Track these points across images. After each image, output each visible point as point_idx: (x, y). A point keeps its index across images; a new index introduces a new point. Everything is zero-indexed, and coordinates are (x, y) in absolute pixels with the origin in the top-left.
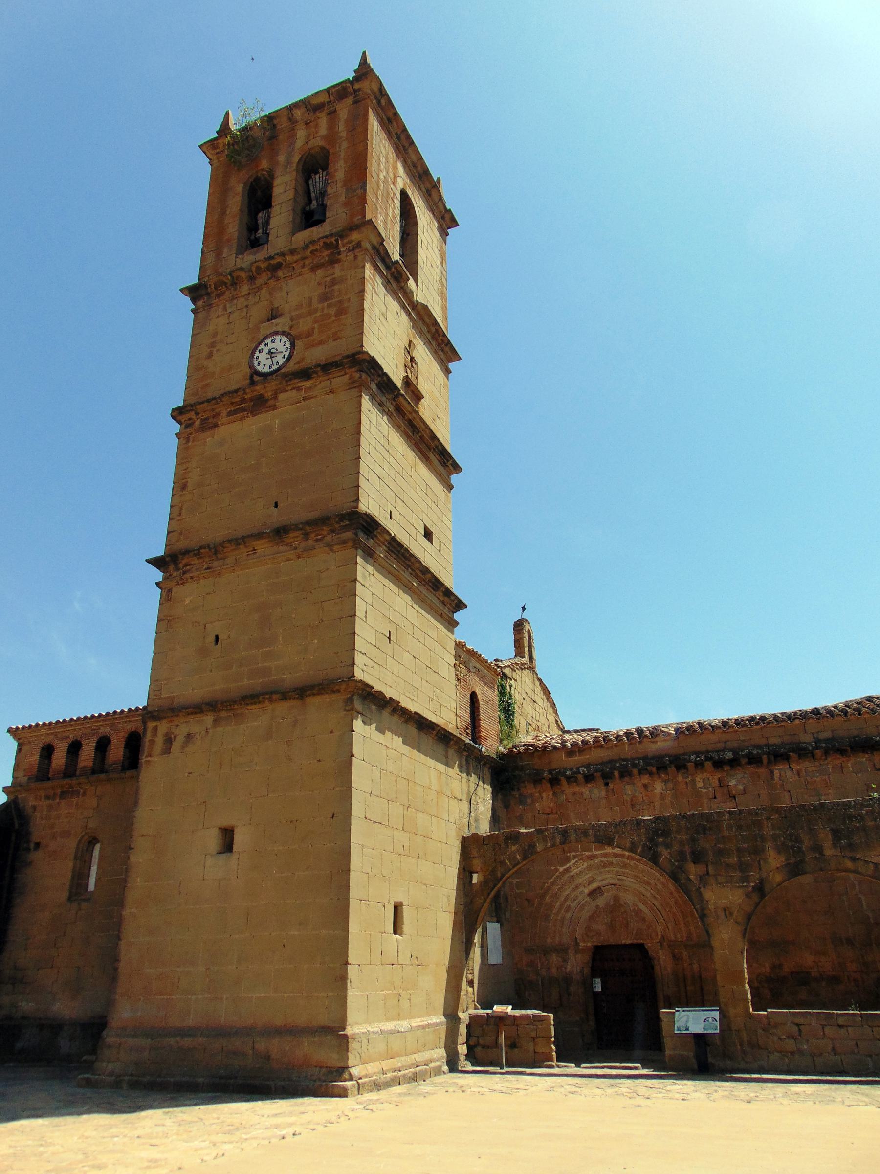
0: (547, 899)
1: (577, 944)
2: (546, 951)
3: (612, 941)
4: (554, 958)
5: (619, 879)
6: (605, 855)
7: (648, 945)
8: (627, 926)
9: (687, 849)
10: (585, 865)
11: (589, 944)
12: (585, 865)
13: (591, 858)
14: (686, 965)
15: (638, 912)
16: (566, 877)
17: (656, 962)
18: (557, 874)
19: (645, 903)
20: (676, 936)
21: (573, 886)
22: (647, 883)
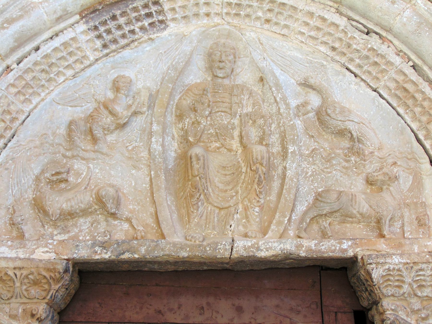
11: (43, 254)
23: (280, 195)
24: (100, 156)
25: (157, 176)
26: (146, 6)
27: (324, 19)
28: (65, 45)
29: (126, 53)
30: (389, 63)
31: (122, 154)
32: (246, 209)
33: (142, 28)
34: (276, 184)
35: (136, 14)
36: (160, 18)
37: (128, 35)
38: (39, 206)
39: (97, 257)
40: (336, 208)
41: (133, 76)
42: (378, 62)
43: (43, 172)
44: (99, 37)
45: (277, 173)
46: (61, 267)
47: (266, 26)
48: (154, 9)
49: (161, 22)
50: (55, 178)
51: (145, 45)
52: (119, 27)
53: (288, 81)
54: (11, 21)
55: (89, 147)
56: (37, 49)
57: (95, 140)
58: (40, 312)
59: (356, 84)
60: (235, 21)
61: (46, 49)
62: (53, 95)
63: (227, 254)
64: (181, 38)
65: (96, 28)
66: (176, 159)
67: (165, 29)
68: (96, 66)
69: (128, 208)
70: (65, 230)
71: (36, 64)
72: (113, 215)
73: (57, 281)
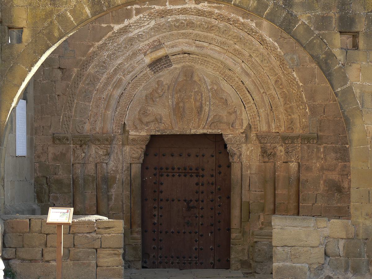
0: (91, 69)
2: (84, 141)
3: (177, 130)
4: (94, 151)
5: (197, 46)
6: (184, 11)
7: (228, 136)
8: (200, 109)
9: (334, 14)
10: (153, 23)
11: (143, 133)
13: (163, 14)
14: (279, 163)
15: (217, 93)
16: (122, 39)
17: (236, 159)
18: (110, 34)
19: (228, 79)
20: (269, 126)
21: (130, 53)
22: (237, 53)
24: (155, 106)
29: (161, 73)
31: (161, 105)
32: (195, 119)
34: (203, 112)
35: (163, 63)
38: (140, 120)
39: (157, 134)
41: (163, 80)
43: (140, 110)
46: (149, 137)
50: (144, 112)
51: (166, 71)
52: (158, 67)
53: (208, 80)
54: (130, 72)
56: (136, 76)
57: (153, 101)
58: (144, 147)
59: (227, 84)
63: (189, 134)
64: (176, 68)
66: (176, 104)
67: (171, 66)
70: (147, 126)
72: (160, 123)
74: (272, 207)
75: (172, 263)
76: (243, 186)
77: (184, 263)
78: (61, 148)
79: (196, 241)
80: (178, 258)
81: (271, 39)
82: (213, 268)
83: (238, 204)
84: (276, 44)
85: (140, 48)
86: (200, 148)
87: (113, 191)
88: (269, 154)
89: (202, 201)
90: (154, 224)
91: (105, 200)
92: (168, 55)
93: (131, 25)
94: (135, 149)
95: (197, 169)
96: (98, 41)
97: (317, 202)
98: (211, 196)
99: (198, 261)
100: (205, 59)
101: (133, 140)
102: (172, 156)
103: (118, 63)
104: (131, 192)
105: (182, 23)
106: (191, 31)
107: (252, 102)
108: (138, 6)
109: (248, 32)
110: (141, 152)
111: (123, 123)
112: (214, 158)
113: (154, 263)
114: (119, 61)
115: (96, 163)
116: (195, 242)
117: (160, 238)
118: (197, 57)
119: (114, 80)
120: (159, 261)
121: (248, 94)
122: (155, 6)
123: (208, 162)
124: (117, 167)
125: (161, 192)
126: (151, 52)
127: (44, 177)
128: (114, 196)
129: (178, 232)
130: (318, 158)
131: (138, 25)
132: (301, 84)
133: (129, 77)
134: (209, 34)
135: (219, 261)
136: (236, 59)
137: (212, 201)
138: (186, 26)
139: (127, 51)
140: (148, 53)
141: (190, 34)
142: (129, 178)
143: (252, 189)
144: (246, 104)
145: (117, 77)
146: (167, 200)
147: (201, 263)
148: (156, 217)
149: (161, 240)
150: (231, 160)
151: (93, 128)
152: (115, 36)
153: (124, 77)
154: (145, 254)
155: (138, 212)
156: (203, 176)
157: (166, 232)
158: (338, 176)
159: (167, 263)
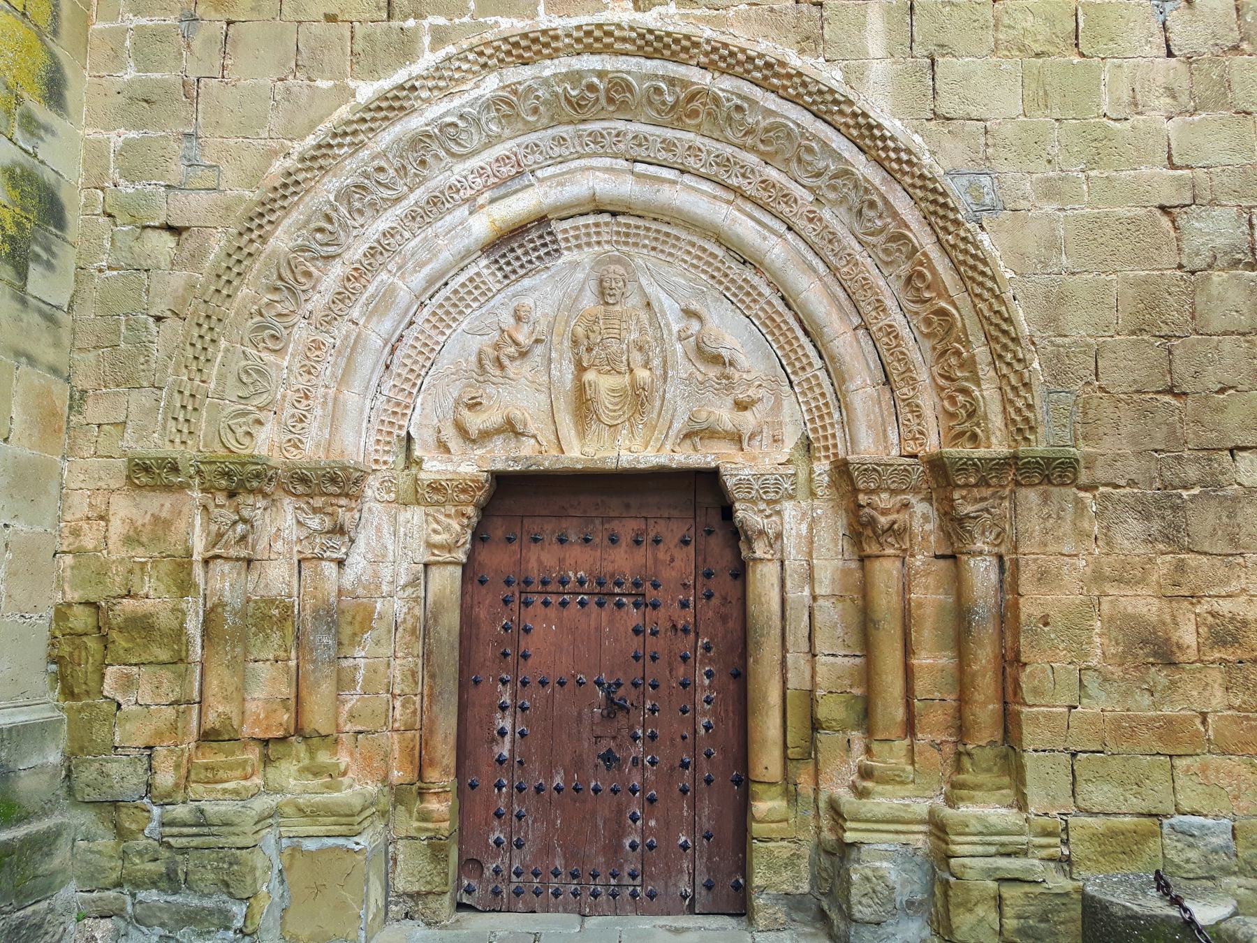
0: (281, 240)
1: (411, 461)
10: (491, 84)
12: (491, 84)
16: (387, 137)
21: (420, 195)
23: (660, 414)
25: (557, 399)
26: (541, 237)
27: (705, 250)
28: (471, 280)
29: (526, 282)
30: (760, 294)
33: (539, 258)
36: (555, 247)
37: (527, 265)
40: (704, 426)
41: (532, 305)
42: (752, 293)
44: (500, 269)
45: (657, 396)
47: (653, 253)
48: (548, 239)
49: (556, 251)
52: (518, 258)
54: (422, 265)
55: (498, 373)
56: (446, 284)
57: (502, 367)
60: (624, 248)
61: (454, 285)
62: (463, 326)
63: (613, 466)
64: (575, 265)
65: (496, 262)
68: (499, 296)
69: (532, 428)
71: (448, 299)
72: (522, 434)
73: (480, 489)
74: (900, 714)
75: (556, 894)
76: (790, 639)
77: (595, 895)
78: (160, 504)
79: (634, 819)
80: (574, 876)
81: (898, 123)
82: (691, 910)
83: (774, 697)
84: (917, 138)
85: (453, 180)
86: (646, 518)
87: (360, 658)
88: (886, 527)
89: (654, 687)
90: (500, 761)
91: (327, 687)
92: (546, 216)
93: (417, 84)
94: (442, 518)
95: (636, 584)
96: (302, 138)
97: (1084, 701)
98: (681, 670)
99: (641, 885)
100: (665, 229)
101: (435, 487)
102: (562, 541)
103: (380, 229)
104: (427, 656)
105: (591, 87)
106: (621, 125)
107: (818, 363)
108: (441, 21)
109: (814, 108)
110: (458, 528)
111: (404, 433)
112: (691, 548)
113: (496, 892)
114: (383, 223)
115: (299, 561)
116: (630, 822)
117: (516, 809)
118: (640, 222)
119: (371, 289)
120: (513, 887)
121: (804, 340)
122: (499, 18)
123: (672, 560)
124: (376, 575)
125: (525, 656)
126: (492, 201)
127: (87, 603)
128: (362, 671)
129: (577, 790)
130: (1082, 535)
131: (440, 89)
132: (1009, 274)
133: (418, 280)
134: (679, 134)
135: (709, 886)
136: (767, 219)
137: (684, 685)
138: (603, 101)
139: (411, 190)
140: (481, 200)
141: (618, 135)
142: (419, 611)
143: (821, 646)
144: (793, 373)
145: (379, 279)
146: (543, 683)
147: (651, 896)
148: (508, 738)
149: (519, 817)
150: (745, 553)
151: (289, 441)
152: (364, 120)
153: (402, 277)
154: (470, 864)
155: (447, 725)
156: (655, 606)
157: (539, 789)
158: (1156, 601)
159: (537, 893)
